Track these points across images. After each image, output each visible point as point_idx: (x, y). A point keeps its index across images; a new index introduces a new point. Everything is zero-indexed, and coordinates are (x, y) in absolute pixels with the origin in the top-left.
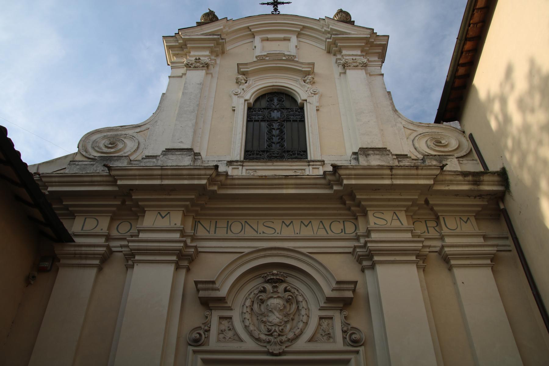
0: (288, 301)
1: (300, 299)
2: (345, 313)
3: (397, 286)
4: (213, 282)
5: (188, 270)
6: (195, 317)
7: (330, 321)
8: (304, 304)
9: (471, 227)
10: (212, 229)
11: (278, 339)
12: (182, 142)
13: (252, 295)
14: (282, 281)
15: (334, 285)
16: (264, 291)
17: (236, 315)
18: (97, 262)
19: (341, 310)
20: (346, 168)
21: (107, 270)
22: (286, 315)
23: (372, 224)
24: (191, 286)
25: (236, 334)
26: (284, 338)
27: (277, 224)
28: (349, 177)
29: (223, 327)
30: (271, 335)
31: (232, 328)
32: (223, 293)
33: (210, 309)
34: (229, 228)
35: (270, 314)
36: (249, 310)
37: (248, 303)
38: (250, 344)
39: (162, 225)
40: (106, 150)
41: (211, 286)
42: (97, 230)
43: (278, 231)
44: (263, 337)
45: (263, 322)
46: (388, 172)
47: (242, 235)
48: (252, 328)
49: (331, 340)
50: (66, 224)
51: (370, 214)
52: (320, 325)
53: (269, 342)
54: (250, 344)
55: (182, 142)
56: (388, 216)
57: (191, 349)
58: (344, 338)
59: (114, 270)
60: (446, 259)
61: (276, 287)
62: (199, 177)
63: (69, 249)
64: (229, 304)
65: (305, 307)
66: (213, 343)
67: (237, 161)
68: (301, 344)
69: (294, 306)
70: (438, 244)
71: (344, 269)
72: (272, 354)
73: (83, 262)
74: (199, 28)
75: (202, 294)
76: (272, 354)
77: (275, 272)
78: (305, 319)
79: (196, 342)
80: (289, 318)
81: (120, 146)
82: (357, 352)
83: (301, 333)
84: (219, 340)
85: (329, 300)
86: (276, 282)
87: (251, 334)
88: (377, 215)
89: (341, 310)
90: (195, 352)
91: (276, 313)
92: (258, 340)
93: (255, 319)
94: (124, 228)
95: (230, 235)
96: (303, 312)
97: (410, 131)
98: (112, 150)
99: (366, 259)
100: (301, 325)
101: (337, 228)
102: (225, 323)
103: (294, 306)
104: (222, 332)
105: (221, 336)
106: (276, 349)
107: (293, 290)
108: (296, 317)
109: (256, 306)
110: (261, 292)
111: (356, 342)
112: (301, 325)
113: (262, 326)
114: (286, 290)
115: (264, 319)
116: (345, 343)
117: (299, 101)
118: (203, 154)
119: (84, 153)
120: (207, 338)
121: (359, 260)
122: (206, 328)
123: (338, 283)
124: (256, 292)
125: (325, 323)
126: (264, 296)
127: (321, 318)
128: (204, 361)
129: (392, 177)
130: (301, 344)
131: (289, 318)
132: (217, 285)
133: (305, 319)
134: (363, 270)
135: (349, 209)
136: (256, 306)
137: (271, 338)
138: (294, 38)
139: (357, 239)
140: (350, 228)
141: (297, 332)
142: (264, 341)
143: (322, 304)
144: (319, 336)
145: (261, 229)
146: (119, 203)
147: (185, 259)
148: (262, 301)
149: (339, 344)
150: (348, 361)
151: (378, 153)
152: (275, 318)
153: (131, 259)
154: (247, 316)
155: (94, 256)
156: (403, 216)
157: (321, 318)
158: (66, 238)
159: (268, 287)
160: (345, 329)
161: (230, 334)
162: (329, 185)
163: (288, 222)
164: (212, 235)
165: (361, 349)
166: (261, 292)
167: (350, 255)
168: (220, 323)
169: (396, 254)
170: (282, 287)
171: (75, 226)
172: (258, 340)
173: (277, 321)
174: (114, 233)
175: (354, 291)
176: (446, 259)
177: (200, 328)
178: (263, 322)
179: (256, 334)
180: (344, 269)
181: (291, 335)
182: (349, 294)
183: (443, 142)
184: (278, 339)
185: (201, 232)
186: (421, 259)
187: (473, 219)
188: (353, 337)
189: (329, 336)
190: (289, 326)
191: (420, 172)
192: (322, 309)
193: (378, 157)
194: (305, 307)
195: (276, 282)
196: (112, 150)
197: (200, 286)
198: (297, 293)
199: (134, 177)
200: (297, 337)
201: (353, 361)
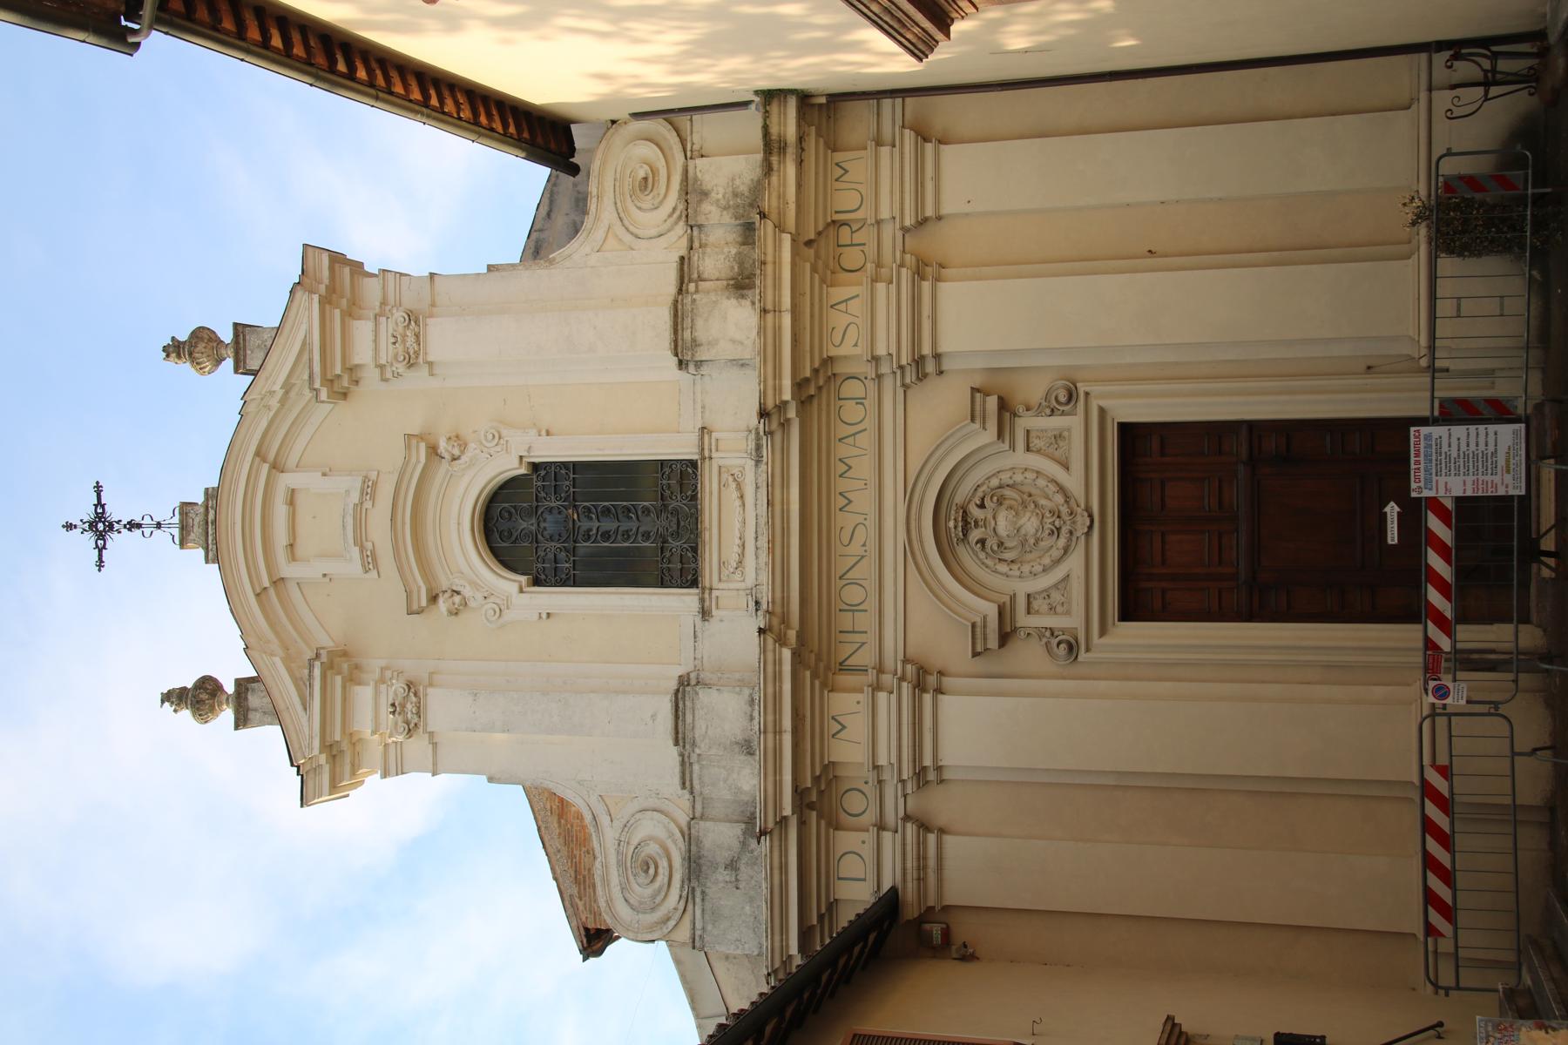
1: (995, 482)
2: (1021, 409)
3: (979, 320)
4: (974, 626)
5: (941, 673)
6: (1028, 654)
7: (1032, 434)
8: (1005, 477)
9: (857, 165)
10: (858, 638)
11: (1066, 518)
12: (653, 717)
13: (989, 562)
15: (977, 426)
16: (982, 542)
17: (1022, 588)
18: (932, 838)
19: (1015, 415)
20: (763, 395)
21: (941, 820)
22: (1024, 505)
23: (858, 351)
24: (979, 665)
25: (1056, 586)
26: (1064, 510)
27: (845, 521)
28: (778, 389)
29: (1045, 608)
30: (1058, 529)
31: (1047, 594)
32: (991, 610)
33: (1015, 630)
34: (853, 609)
35: (1023, 532)
36: (1015, 567)
37: (1003, 568)
38: (1075, 563)
39: (863, 730)
40: (662, 878)
41: (978, 630)
42: (868, 852)
43: (860, 519)
44: (1062, 542)
46: (770, 317)
47: (871, 585)
48: (1047, 561)
49: (1066, 434)
50: (845, 917)
51: (833, 352)
52: (1039, 451)
53: (1071, 533)
54: (1075, 563)
55: (653, 717)
56: (838, 320)
57: (1083, 656)
58: (1063, 413)
59: (939, 805)
60: (922, 222)
61: (976, 522)
62: (778, 662)
63: (910, 894)
64: (1007, 599)
65: (1009, 474)
66: (1072, 621)
67: (702, 600)
68: (1073, 482)
69: (1007, 492)
70: (888, 231)
71: (941, 404)
72: (1091, 527)
73: (932, 862)
74: (285, 716)
75: (993, 642)
76: (1091, 527)
77: (951, 524)
79: (1072, 648)
80: (1028, 501)
81: (652, 849)
82: (1087, 394)
84: (1068, 613)
85: (1000, 435)
86: (967, 525)
88: (837, 338)
89: (1015, 415)
90: (1088, 650)
91: (1021, 522)
92: (1066, 550)
93: (1029, 556)
94: (854, 803)
95: (872, 604)
96: (1019, 478)
97: (611, 242)
98: (663, 864)
99: (923, 366)
100: (1041, 482)
101: (851, 412)
102: (1035, 605)
103: (1007, 492)
104: (1052, 609)
105: (1059, 609)
107: (980, 494)
108: (1026, 489)
109: (1008, 556)
111: (1071, 396)
112: (1041, 482)
113: (1042, 544)
114: (982, 506)
115: (1032, 541)
116: (1072, 413)
117: (523, 471)
118: (681, 671)
119: (672, 923)
120: (1063, 631)
121: (922, 376)
122: (1048, 634)
123: (973, 420)
124: (982, 555)
125: (1036, 443)
126: (992, 543)
127: (1028, 449)
128: (1103, 632)
129: (777, 310)
130: (1073, 482)
131: (1028, 501)
132: (978, 620)
135: (820, 388)
136: (1008, 556)
137: (1064, 530)
138: (286, 481)
139: (879, 377)
140: (852, 389)
141: (1053, 488)
142: (1070, 540)
144: (1057, 454)
145: (855, 549)
146: (814, 814)
147: (924, 680)
148: (1001, 544)
149: (1072, 423)
151: (688, 322)
152: (1030, 524)
153: (924, 776)
154: (1026, 568)
155: (921, 844)
156: (838, 293)
157: (1028, 449)
158: (890, 904)
159: (975, 535)
160: (1048, 411)
161: (1056, 596)
162: (785, 425)
163: (842, 502)
164: (871, 638)
165: (1082, 388)
167: (909, 393)
168: (1037, 612)
169: (917, 317)
170: (976, 513)
171: (857, 895)
172: (1066, 550)
173: (1035, 522)
174: (870, 817)
176: (922, 222)
179: (1056, 553)
180: (941, 404)
181: (1059, 499)
182: (992, 403)
183: (642, 174)
184: (1066, 518)
185: (866, 657)
186: (925, 269)
187: (839, 157)
188: (1063, 399)
189: (1058, 437)
190: (1043, 502)
191: (770, 258)
192: (1013, 447)
193: (699, 323)
194: (1009, 474)
195: (967, 525)
196: (663, 864)
197: (979, 649)
198: (984, 488)
199: (778, 785)
200: (1062, 489)
201: (1103, 403)
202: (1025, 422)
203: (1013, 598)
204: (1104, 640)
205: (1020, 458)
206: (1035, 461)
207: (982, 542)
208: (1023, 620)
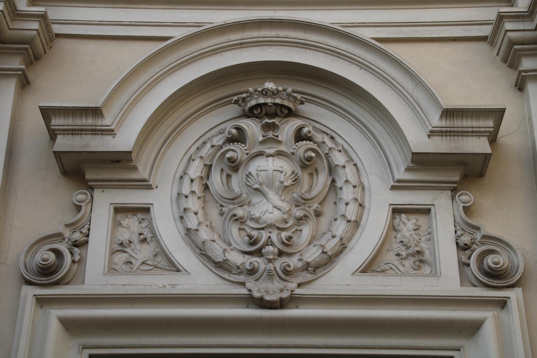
0: (306, 164)
1: (339, 159)
2: (466, 197)
4: (96, 112)
5: (24, 83)
7: (422, 220)
8: (349, 173)
11: (279, 264)
13: (206, 151)
14: (291, 113)
15: (436, 121)
16: (239, 137)
19: (454, 190)
22: (303, 201)
25: (161, 251)
26: (293, 262)
29: (124, 235)
30: (259, 253)
32: (124, 140)
33: (90, 187)
35: (256, 199)
36: (197, 187)
37: (196, 170)
38: (200, 279)
41: (89, 121)
44: (236, 258)
45: (236, 219)
48: (204, 234)
49: (427, 270)
52: (393, 228)
53: (252, 272)
54: (200, 279)
57: (30, 292)
58: (463, 265)
61: (273, 127)
64: (143, 173)
65: (354, 180)
66: (96, 274)
68: (340, 278)
69: (322, 179)
72: (262, 303)
75: (63, 143)
76: (262, 303)
77: (270, 85)
78: (351, 212)
79: (47, 273)
80: (307, 210)
82: (503, 304)
83: (342, 248)
84: (112, 269)
85: (421, 161)
86: (271, 114)
87: (202, 253)
89: (454, 190)
90: (41, 301)
91: (272, 195)
92: (222, 266)
93: (214, 212)
96: (347, 194)
100: (340, 228)
102: (132, 225)
103: (322, 179)
105: (120, 258)
106: (272, 290)
107: (319, 137)
108: (328, 210)
109: (216, 180)
110: (231, 140)
111: (496, 276)
112: (340, 228)
113: (234, 229)
115: (240, 212)
116: (464, 279)
120: (80, 262)
122: (77, 236)
123: (449, 113)
124: (218, 141)
125: (408, 225)
126: (238, 151)
127: (397, 211)
128: (71, 326)
130: (340, 278)
131: (307, 210)
132: (107, 121)
133: (351, 212)
134: (520, 86)
136: (216, 180)
137: (259, 262)
141: (331, 245)
142: (239, 270)
143: (401, 174)
144: (390, 257)
148: (234, 166)
149: (447, 279)
150: (473, 328)
152: (269, 208)
154: (193, 204)
157: (397, 211)
159: (253, 128)
160: (466, 239)
161: (144, 252)
165: (514, 296)
166: (231, 140)
167: (483, 46)
168: (117, 224)
170: (288, 129)
172: (222, 266)
173: (274, 216)
175: (493, 139)
177: (58, 236)
178: (236, 219)
179: (217, 251)
181: (312, 255)
182: (481, 146)
188: (490, 260)
189: (420, 259)
190: (307, 231)
192: (399, 186)
194: (354, 180)
195: (271, 114)
197: (57, 122)
198: (329, 143)
200: (329, 260)
201: (489, 330)
202: (445, 213)
203: (144, 185)
204: (54, 328)
205: (380, 201)
206: (376, 222)
207: (239, 137)
208: (103, 203)
